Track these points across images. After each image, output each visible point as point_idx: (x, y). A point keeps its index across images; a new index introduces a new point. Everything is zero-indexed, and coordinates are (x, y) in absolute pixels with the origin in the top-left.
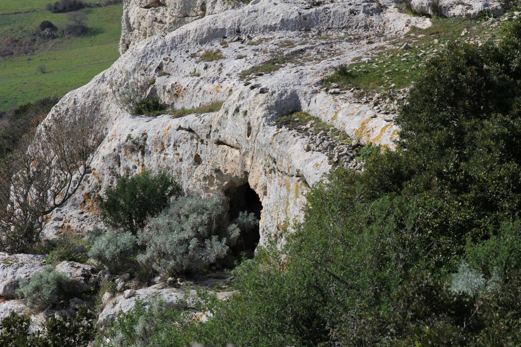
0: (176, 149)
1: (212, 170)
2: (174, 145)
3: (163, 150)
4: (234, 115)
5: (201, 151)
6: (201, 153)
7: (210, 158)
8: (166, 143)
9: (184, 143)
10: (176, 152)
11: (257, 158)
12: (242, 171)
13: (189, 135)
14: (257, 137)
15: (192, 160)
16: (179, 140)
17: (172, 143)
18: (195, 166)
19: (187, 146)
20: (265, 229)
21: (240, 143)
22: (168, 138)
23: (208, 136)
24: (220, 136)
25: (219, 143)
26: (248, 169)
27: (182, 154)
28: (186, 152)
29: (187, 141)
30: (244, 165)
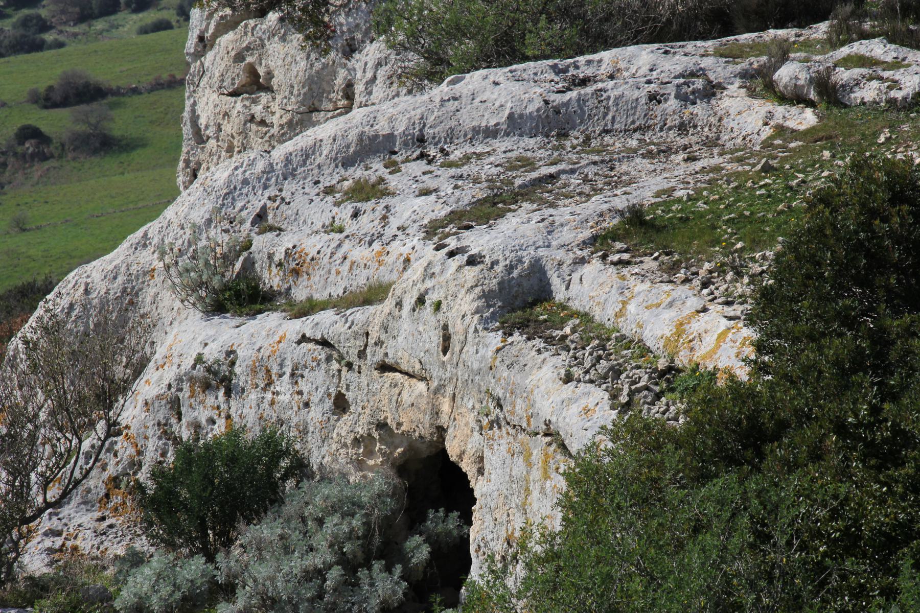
0: (296, 383)
2: (293, 375)
5: (348, 386)
6: (348, 389)
7: (365, 399)
8: (275, 370)
10: (296, 388)
12: (432, 424)
13: (321, 353)
15: (329, 404)
17: (288, 370)
18: (336, 417)
19: (319, 376)
20: (482, 545)
24: (386, 355)
28: (317, 388)
29: (318, 364)
30: (437, 413)
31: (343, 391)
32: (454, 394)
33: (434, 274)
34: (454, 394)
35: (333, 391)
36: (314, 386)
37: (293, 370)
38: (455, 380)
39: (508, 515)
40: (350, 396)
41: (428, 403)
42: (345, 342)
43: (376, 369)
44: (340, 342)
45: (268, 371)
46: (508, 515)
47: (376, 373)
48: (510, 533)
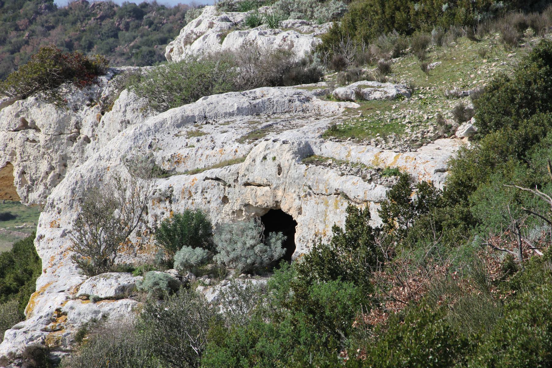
3: (190, 197)
5: (229, 193)
8: (193, 191)
9: (212, 189)
10: (204, 197)
13: (216, 183)
14: (289, 174)
15: (220, 201)
17: (200, 191)
20: (302, 238)
21: (270, 181)
23: (236, 180)
24: (248, 179)
25: (247, 184)
26: (278, 199)
27: (210, 198)
35: (222, 196)
40: (229, 197)
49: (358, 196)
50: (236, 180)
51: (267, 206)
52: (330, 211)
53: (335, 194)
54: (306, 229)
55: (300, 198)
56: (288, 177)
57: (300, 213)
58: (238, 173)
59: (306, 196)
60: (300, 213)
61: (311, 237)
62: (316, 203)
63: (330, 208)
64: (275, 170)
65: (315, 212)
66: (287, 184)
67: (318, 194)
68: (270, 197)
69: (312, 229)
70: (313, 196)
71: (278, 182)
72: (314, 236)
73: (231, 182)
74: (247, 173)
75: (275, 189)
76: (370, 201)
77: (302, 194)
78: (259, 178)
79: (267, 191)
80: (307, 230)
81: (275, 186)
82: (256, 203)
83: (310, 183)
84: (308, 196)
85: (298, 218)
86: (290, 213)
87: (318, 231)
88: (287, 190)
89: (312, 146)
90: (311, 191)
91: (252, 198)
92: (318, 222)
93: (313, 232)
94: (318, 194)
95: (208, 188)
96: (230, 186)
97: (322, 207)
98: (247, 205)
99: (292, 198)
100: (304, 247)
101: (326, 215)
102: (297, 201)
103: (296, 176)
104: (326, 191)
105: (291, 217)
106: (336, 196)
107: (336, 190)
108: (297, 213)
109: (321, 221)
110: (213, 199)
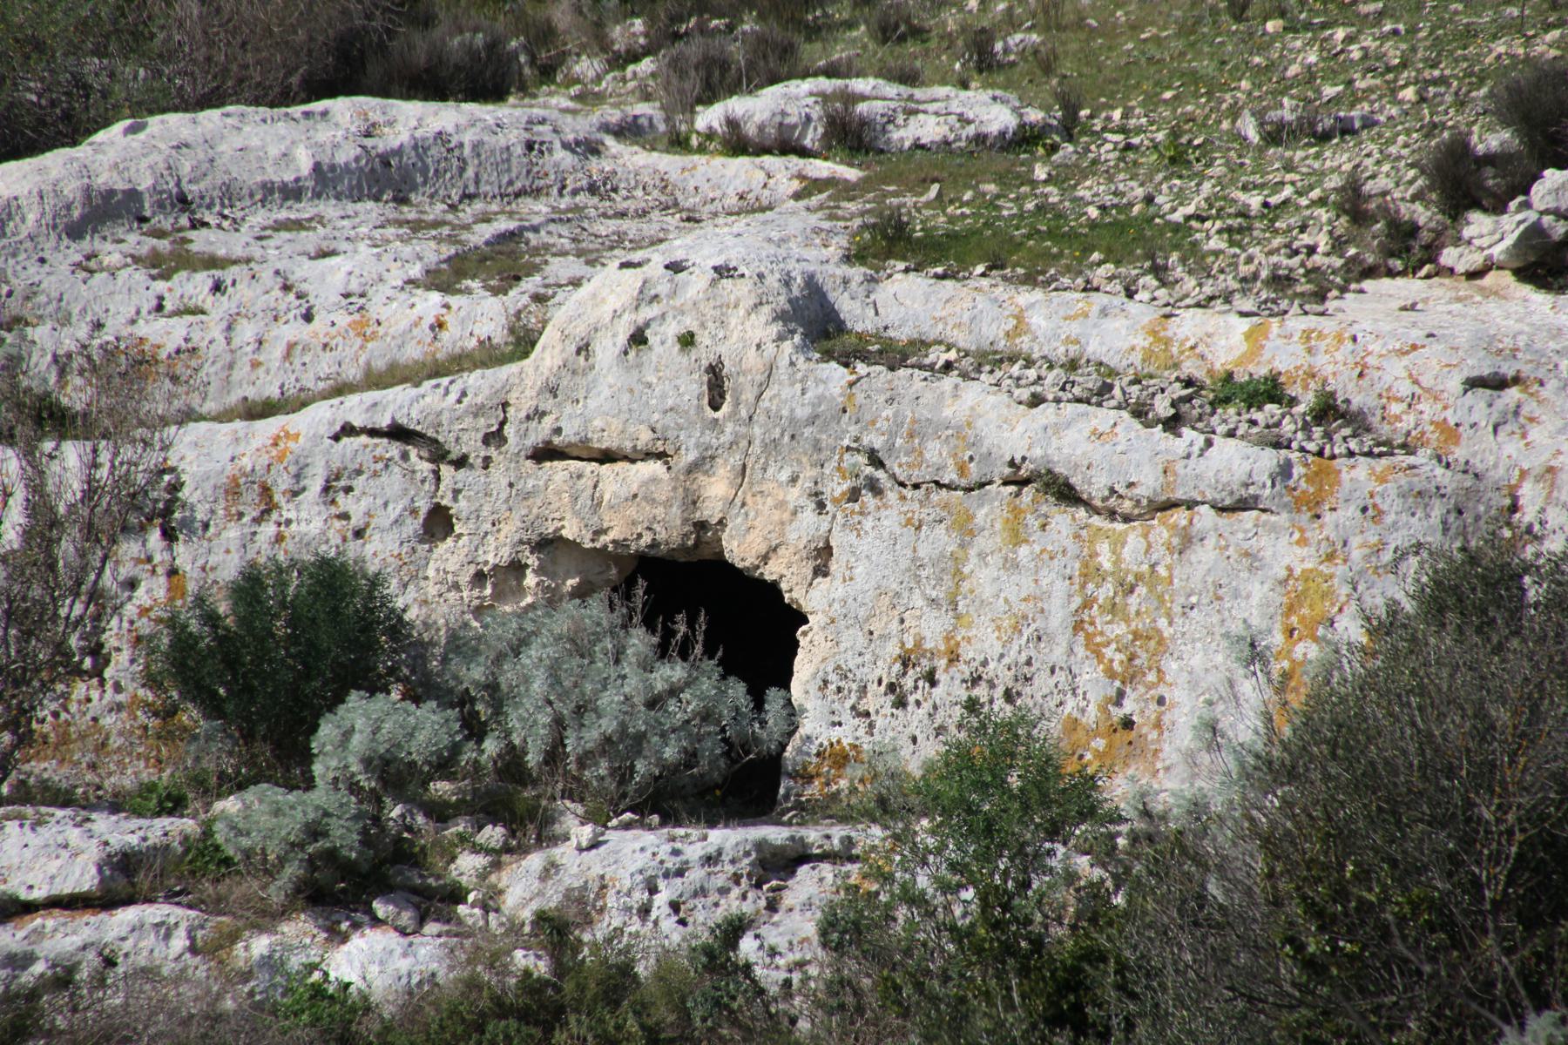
0: (333, 502)
1: (521, 542)
2: (326, 489)
3: (267, 512)
4: (626, 353)
5: (456, 492)
6: (455, 499)
7: (505, 507)
8: (282, 483)
9: (375, 474)
10: (333, 510)
11: (765, 470)
12: (685, 521)
13: (394, 449)
14: (764, 404)
15: (413, 526)
16: (352, 466)
17: (315, 486)
18: (427, 547)
19: (393, 481)
20: (833, 677)
21: (671, 434)
22: (293, 469)
23: (495, 438)
24: (558, 431)
25: (546, 453)
26: (710, 511)
27: (368, 514)
28: (386, 505)
29: (387, 466)
30: (694, 503)
31: (444, 502)
32: (744, 467)
33: (656, 296)
34: (744, 467)
35: (423, 506)
36: (379, 501)
37: (327, 481)
38: (744, 443)
39: (902, 621)
40: (461, 507)
41: (675, 489)
42: (451, 423)
43: (528, 458)
44: (440, 424)
45: (266, 491)
46: (902, 621)
47: (529, 463)
48: (909, 645)
49: (1131, 485)
50: (495, 438)
51: (654, 544)
52: (982, 556)
53: (1006, 483)
54: (853, 638)
55: (821, 506)
56: (760, 417)
57: (821, 571)
58: (505, 405)
59: (854, 495)
60: (821, 571)
61: (881, 670)
62: (909, 522)
63: (982, 542)
64: (693, 387)
65: (904, 563)
66: (756, 448)
67: (916, 486)
68: (667, 504)
69: (885, 637)
70: (892, 496)
71: (709, 438)
72: (897, 667)
73: (471, 445)
74: (548, 404)
75: (693, 468)
76: (1191, 505)
77: (837, 487)
78: (616, 424)
79: (654, 480)
80: (861, 640)
81: (692, 456)
82: (598, 533)
83: (878, 442)
84: (867, 497)
85: (814, 593)
86: (770, 572)
87: (919, 643)
88: (754, 473)
89: (832, 296)
90: (880, 474)
91: (577, 514)
92: (917, 600)
93: (893, 649)
94: (916, 486)
95: (359, 472)
96: (461, 463)
97: (939, 540)
98: (549, 545)
99: (781, 505)
100: (846, 717)
101: (959, 577)
102: (809, 516)
103: (802, 413)
104: (962, 470)
105: (773, 589)
106: (1012, 488)
107: (1012, 463)
108: (809, 572)
109: (933, 602)
110: (384, 519)
